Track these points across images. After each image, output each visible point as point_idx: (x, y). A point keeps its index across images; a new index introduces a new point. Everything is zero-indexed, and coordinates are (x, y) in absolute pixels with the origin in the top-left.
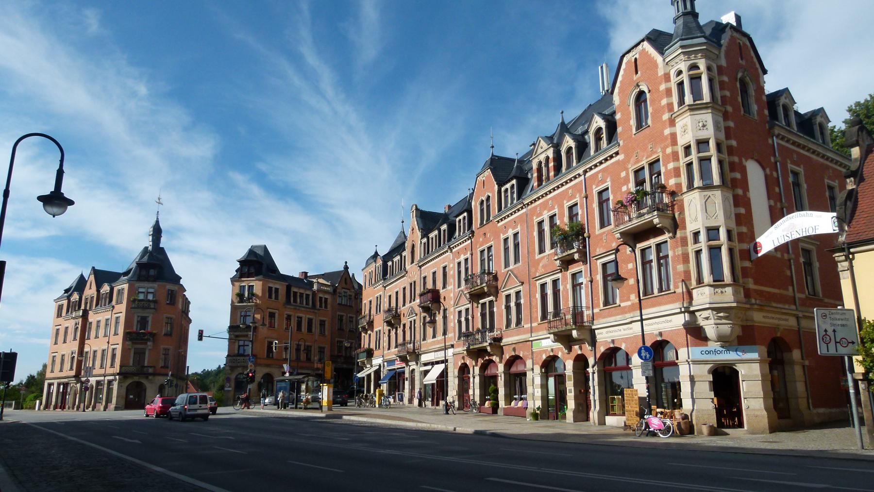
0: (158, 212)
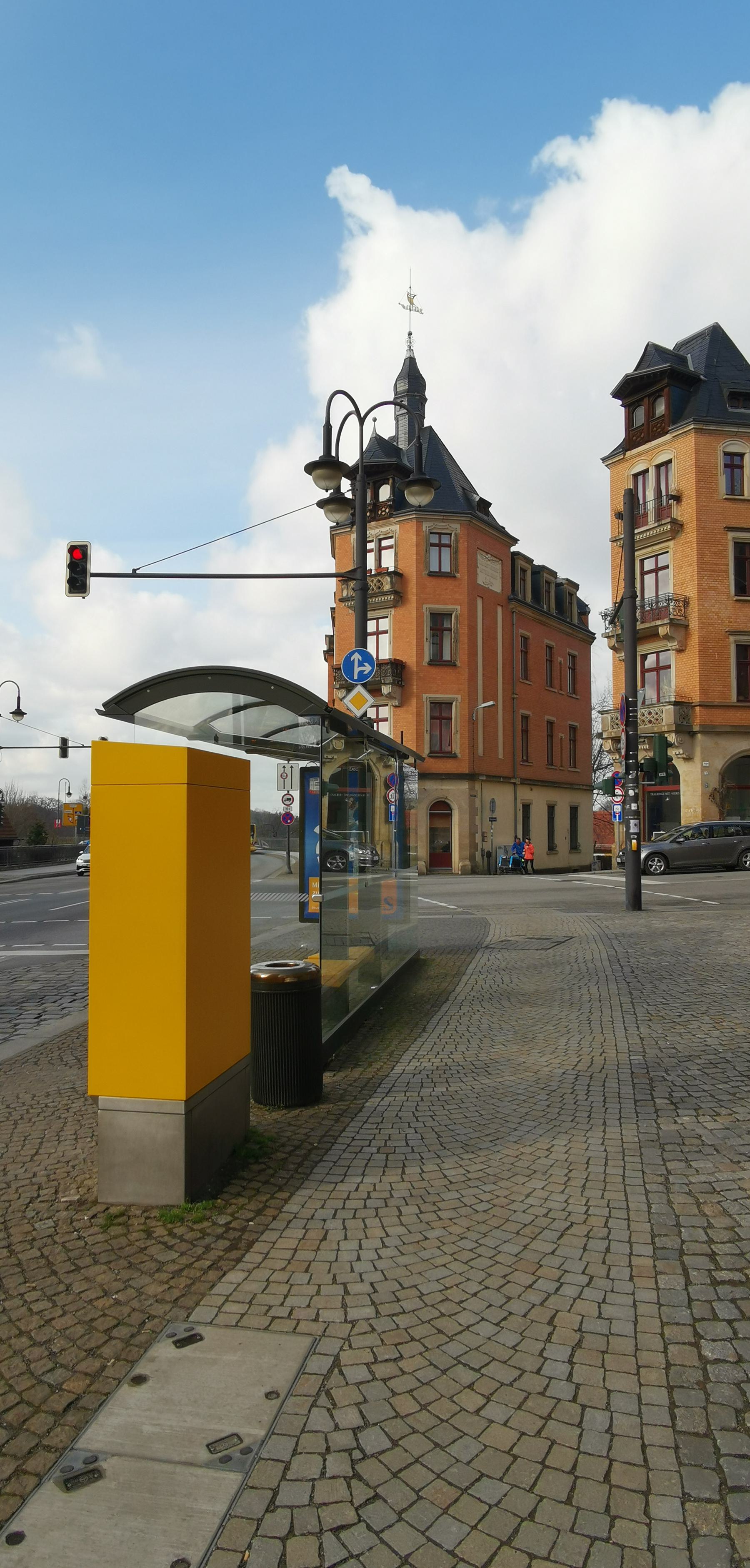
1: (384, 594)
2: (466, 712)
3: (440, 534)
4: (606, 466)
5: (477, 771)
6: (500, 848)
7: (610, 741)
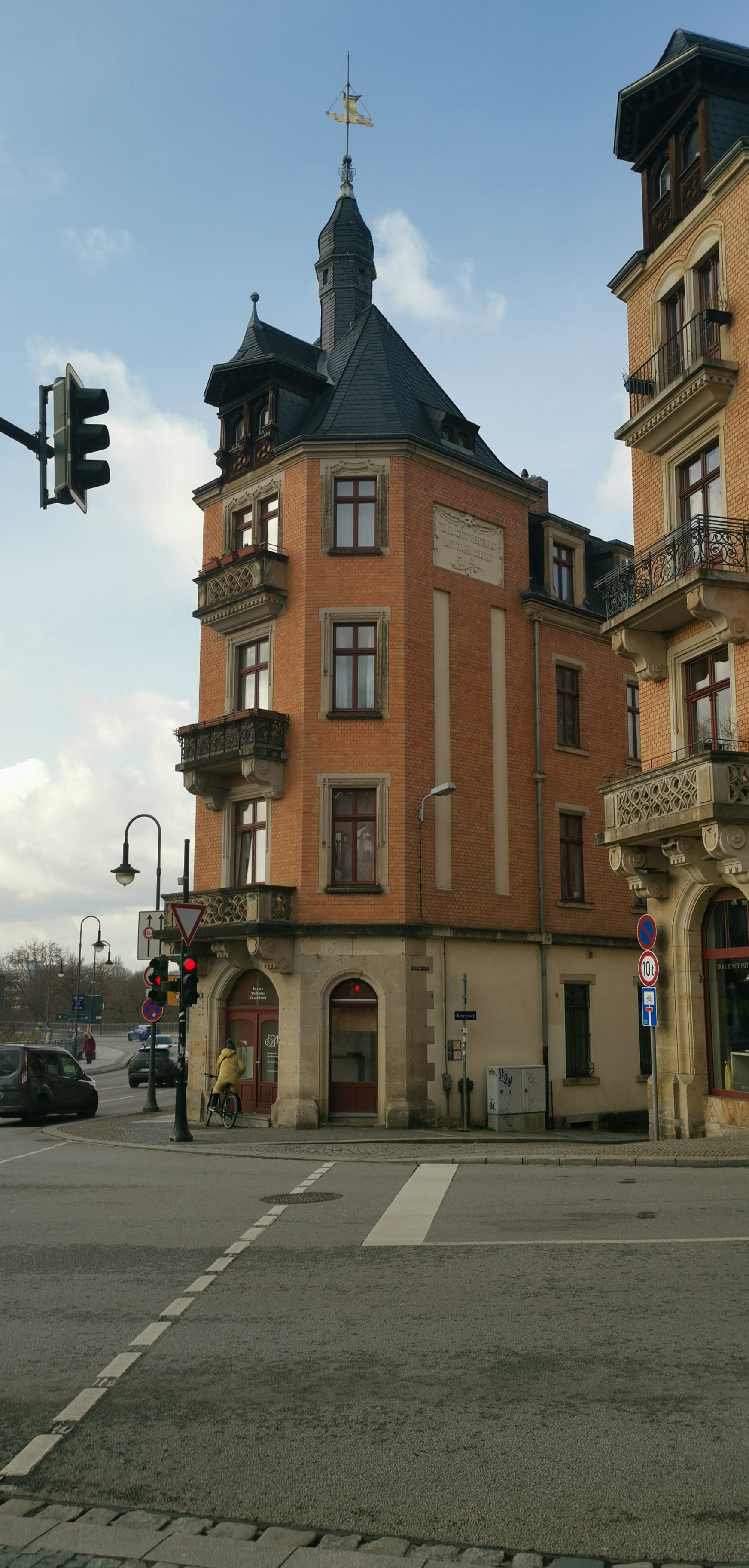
0: (348, 161)
1: (250, 594)
2: (402, 805)
3: (356, 480)
4: (620, 297)
5: (431, 920)
6: (492, 1072)
7: (619, 850)
